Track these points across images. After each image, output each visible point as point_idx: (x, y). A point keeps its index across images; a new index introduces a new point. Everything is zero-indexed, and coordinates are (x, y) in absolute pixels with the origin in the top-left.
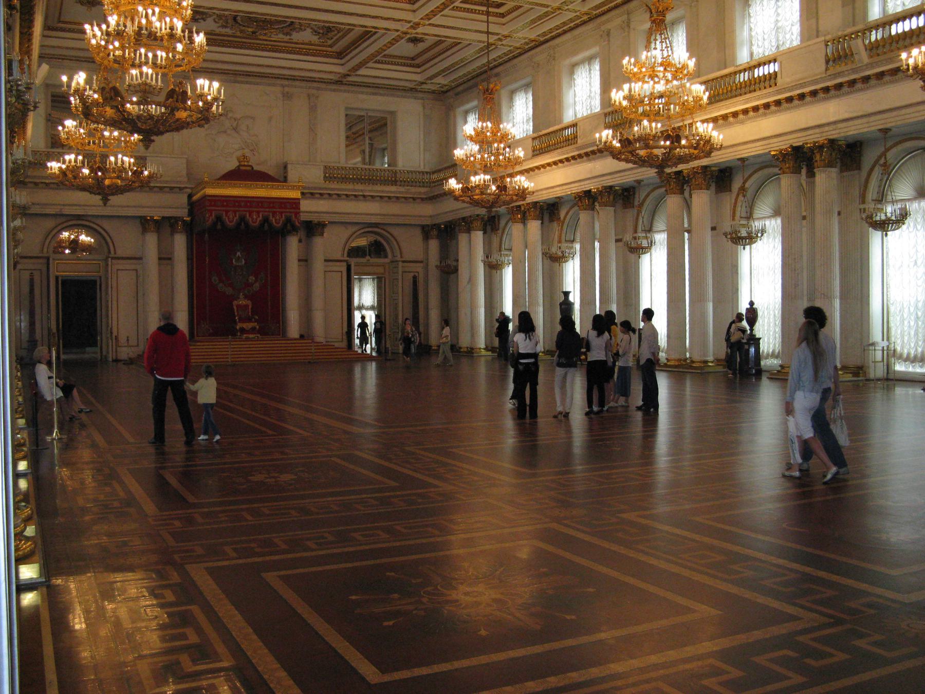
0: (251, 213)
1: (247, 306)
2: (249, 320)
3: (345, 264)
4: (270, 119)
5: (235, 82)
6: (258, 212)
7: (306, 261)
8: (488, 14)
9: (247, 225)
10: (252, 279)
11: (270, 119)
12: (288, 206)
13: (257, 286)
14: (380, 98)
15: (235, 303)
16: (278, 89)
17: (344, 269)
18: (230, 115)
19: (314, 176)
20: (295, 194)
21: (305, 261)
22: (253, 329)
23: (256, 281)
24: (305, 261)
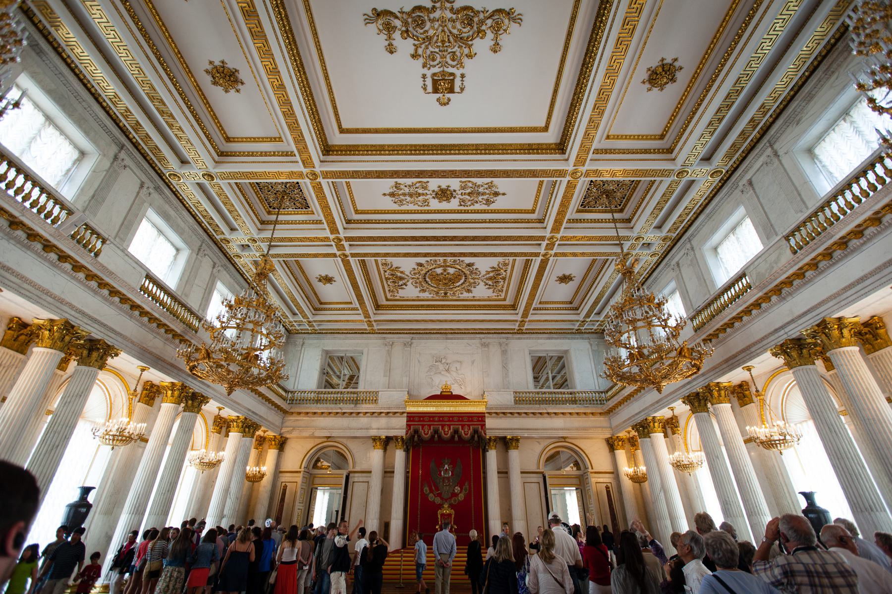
0: (443, 426)
1: (450, 515)
3: (541, 475)
5: (447, 339)
6: (449, 426)
7: (507, 473)
8: (614, 221)
9: (440, 437)
10: (457, 489)
11: (473, 362)
12: (475, 419)
13: (461, 497)
14: (553, 341)
15: (439, 512)
16: (477, 341)
17: (541, 480)
18: (443, 361)
19: (506, 399)
20: (481, 409)
21: (504, 473)
24: (504, 473)
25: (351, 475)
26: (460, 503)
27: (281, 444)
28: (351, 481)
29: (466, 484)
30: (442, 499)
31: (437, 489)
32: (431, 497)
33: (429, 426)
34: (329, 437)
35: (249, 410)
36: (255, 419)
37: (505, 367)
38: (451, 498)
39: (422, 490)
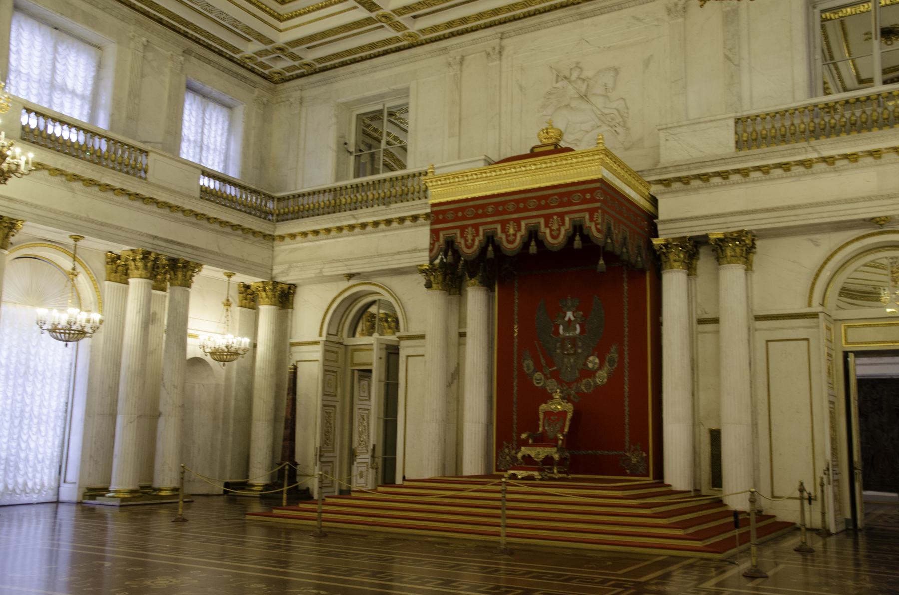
0: (504, 223)
1: (563, 413)
2: (553, 442)
4: (647, 63)
10: (593, 361)
11: (647, 63)
13: (602, 377)
15: (543, 407)
22: (548, 460)
23: (600, 368)
25: (403, 344)
26: (599, 389)
27: (284, 297)
28: (403, 354)
29: (613, 349)
30: (561, 382)
31: (551, 363)
32: (538, 379)
33: (476, 227)
34: (350, 276)
35: (155, 237)
36: (182, 254)
37: (731, 59)
38: (578, 380)
39: (520, 366)
